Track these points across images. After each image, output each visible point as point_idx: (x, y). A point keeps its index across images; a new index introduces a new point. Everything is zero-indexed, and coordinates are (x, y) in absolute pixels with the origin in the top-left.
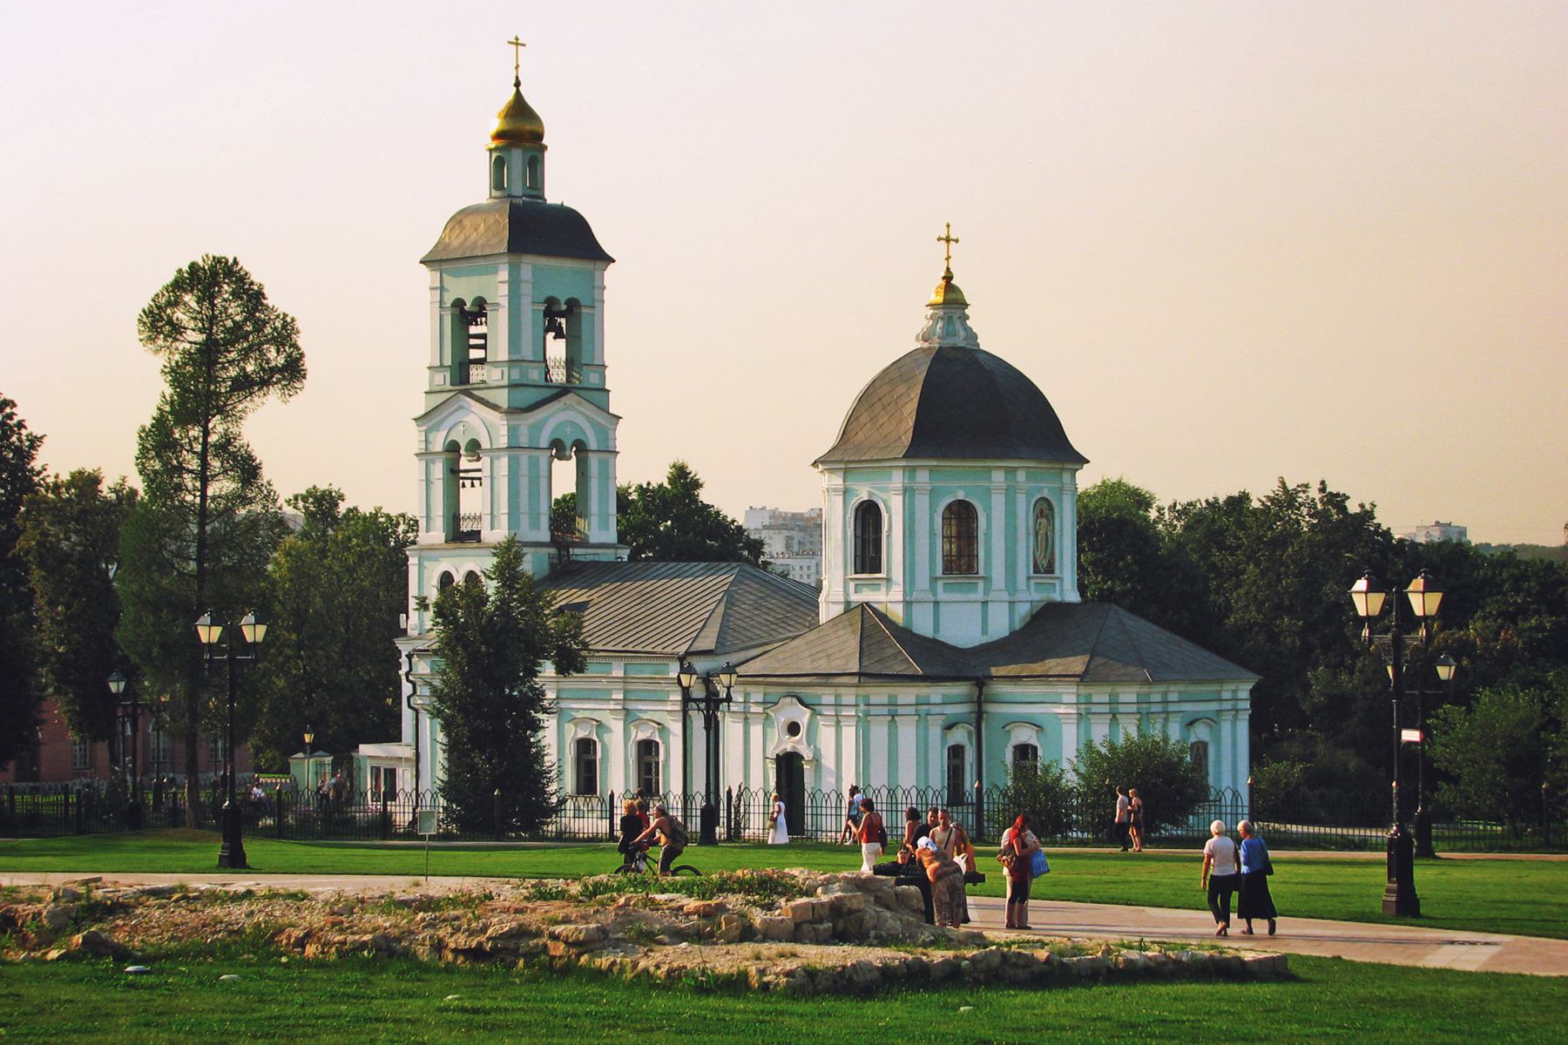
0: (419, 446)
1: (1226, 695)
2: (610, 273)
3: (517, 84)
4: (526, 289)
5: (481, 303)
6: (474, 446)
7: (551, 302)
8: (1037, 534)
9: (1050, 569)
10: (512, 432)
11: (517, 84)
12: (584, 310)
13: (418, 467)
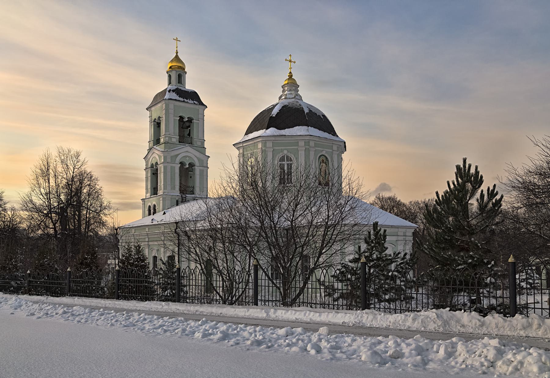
0: (144, 167)
1: (399, 234)
2: (206, 112)
3: (177, 53)
4: (171, 111)
5: (159, 117)
6: (157, 163)
7: (181, 118)
8: (320, 169)
9: (327, 184)
10: (165, 158)
11: (177, 53)
12: (194, 121)
13: (144, 172)
